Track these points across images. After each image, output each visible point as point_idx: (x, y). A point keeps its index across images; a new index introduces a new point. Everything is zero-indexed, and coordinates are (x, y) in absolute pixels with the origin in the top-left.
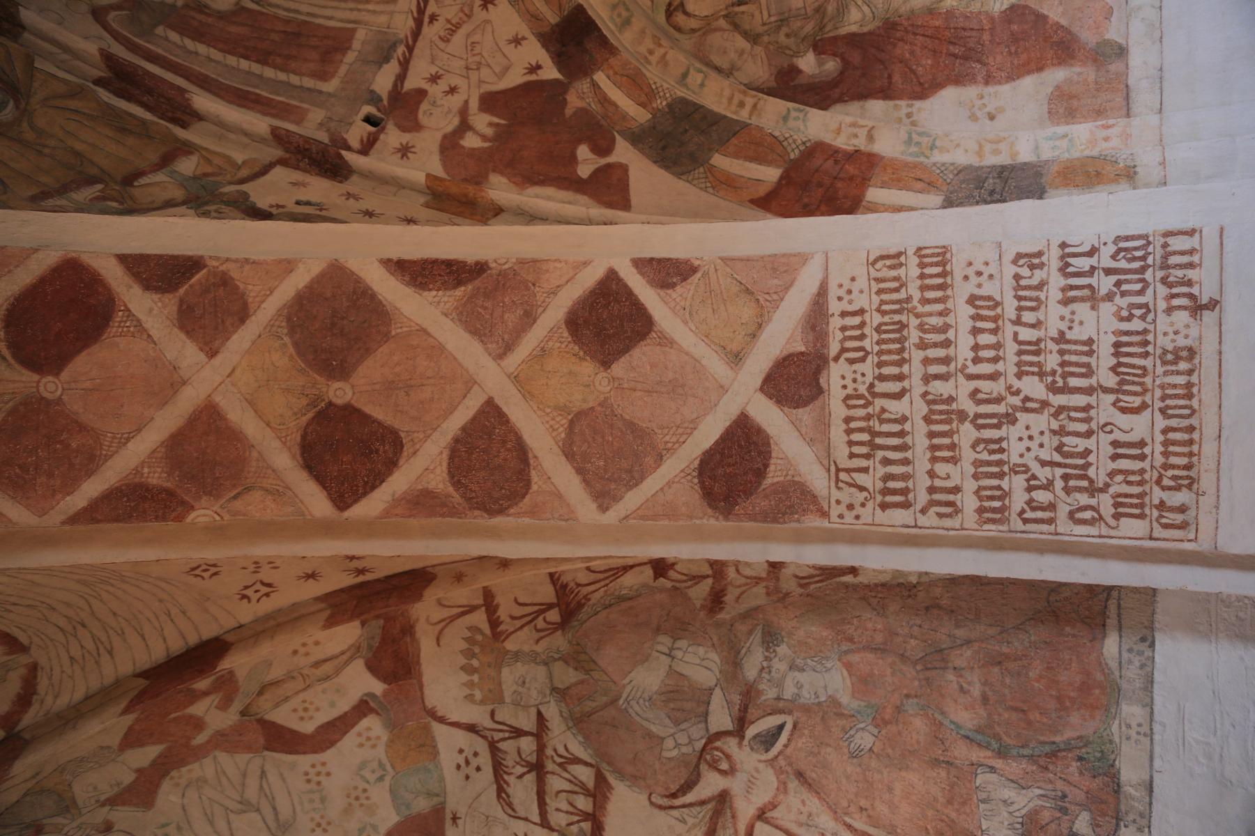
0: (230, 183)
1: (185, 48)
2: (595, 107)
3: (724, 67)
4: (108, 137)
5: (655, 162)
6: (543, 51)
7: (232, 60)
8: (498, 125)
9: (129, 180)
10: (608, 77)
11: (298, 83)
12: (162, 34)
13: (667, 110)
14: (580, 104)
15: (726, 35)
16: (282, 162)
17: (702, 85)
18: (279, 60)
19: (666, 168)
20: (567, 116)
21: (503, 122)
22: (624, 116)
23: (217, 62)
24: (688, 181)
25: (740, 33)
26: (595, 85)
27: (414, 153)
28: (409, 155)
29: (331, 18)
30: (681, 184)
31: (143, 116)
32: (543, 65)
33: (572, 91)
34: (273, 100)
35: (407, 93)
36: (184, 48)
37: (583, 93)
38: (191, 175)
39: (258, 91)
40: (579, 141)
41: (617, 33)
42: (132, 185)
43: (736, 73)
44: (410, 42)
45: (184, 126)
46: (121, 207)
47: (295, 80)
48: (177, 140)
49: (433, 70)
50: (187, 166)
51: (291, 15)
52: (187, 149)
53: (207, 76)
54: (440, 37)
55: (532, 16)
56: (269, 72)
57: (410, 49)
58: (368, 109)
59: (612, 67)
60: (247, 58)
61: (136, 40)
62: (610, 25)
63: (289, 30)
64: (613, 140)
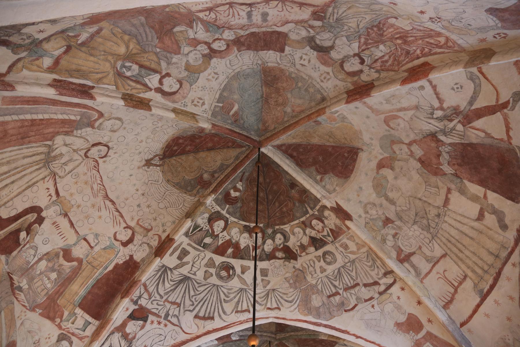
0: (24, 58)
1: (67, 115)
4: (83, 66)
7: (46, 116)
9: (69, 48)
11: (13, 116)
12: (77, 117)
16: (4, 75)
18: (26, 124)
23: (52, 113)
29: (11, 151)
31: (72, 79)
34: (21, 105)
36: (67, 114)
38: (44, 58)
39: (30, 106)
42: (67, 46)
45: (55, 80)
46: (68, 33)
47: (15, 117)
48: (55, 73)
50: (47, 62)
51: (29, 146)
52: (51, 70)
53: (54, 105)
56: (28, 117)
60: (41, 120)
61: (85, 110)
63: (27, 139)
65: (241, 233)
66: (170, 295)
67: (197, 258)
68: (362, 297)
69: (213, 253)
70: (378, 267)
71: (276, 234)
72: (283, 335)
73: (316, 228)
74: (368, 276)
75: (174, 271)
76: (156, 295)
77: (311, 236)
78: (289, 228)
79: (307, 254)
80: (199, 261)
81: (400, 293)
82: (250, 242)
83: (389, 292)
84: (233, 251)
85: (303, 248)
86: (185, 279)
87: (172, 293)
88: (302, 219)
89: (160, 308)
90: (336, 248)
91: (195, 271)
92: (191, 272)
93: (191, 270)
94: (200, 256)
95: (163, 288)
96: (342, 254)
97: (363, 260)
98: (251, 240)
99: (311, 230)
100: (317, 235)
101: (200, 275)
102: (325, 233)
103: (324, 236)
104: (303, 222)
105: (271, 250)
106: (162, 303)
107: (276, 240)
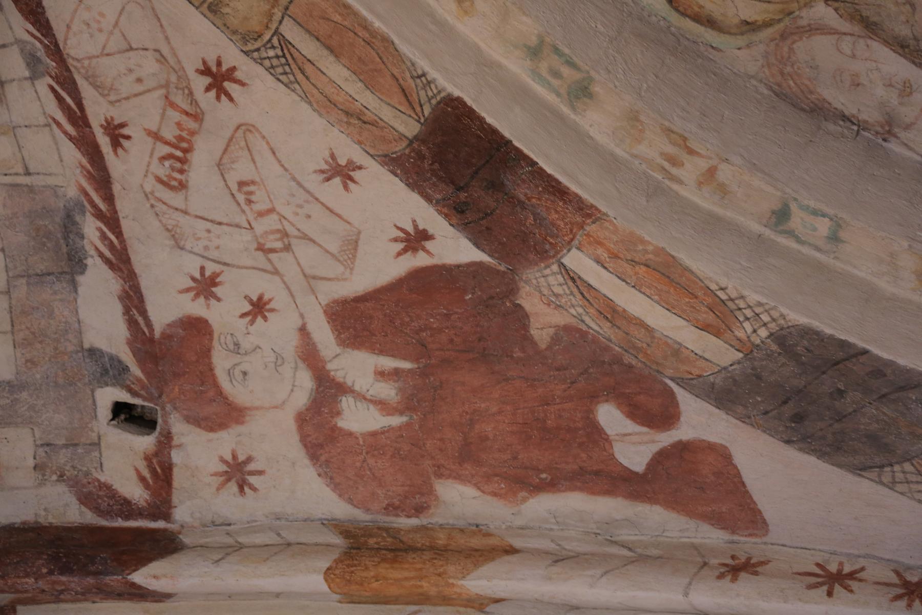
2: (595, 325)
3: (863, 116)
5: (788, 442)
6: (415, 199)
8: (396, 373)
10: (598, 261)
13: (774, 347)
14: (558, 319)
15: (846, 45)
17: (834, 238)
19: (821, 455)
20: (543, 346)
21: (406, 365)
22: (677, 351)
24: (881, 483)
25: (886, 43)
26: (573, 278)
27: (260, 473)
28: (252, 479)
30: (865, 486)
32: (431, 231)
33: (525, 289)
35: (166, 336)
37: (557, 296)
40: (594, 397)
41: (565, 110)
43: (902, 135)
44: (102, 206)
49: (192, 265)
54: (159, 180)
55: (347, 113)
57: (112, 221)
58: (108, 396)
59: (600, 243)
62: (538, 89)
64: (672, 394)
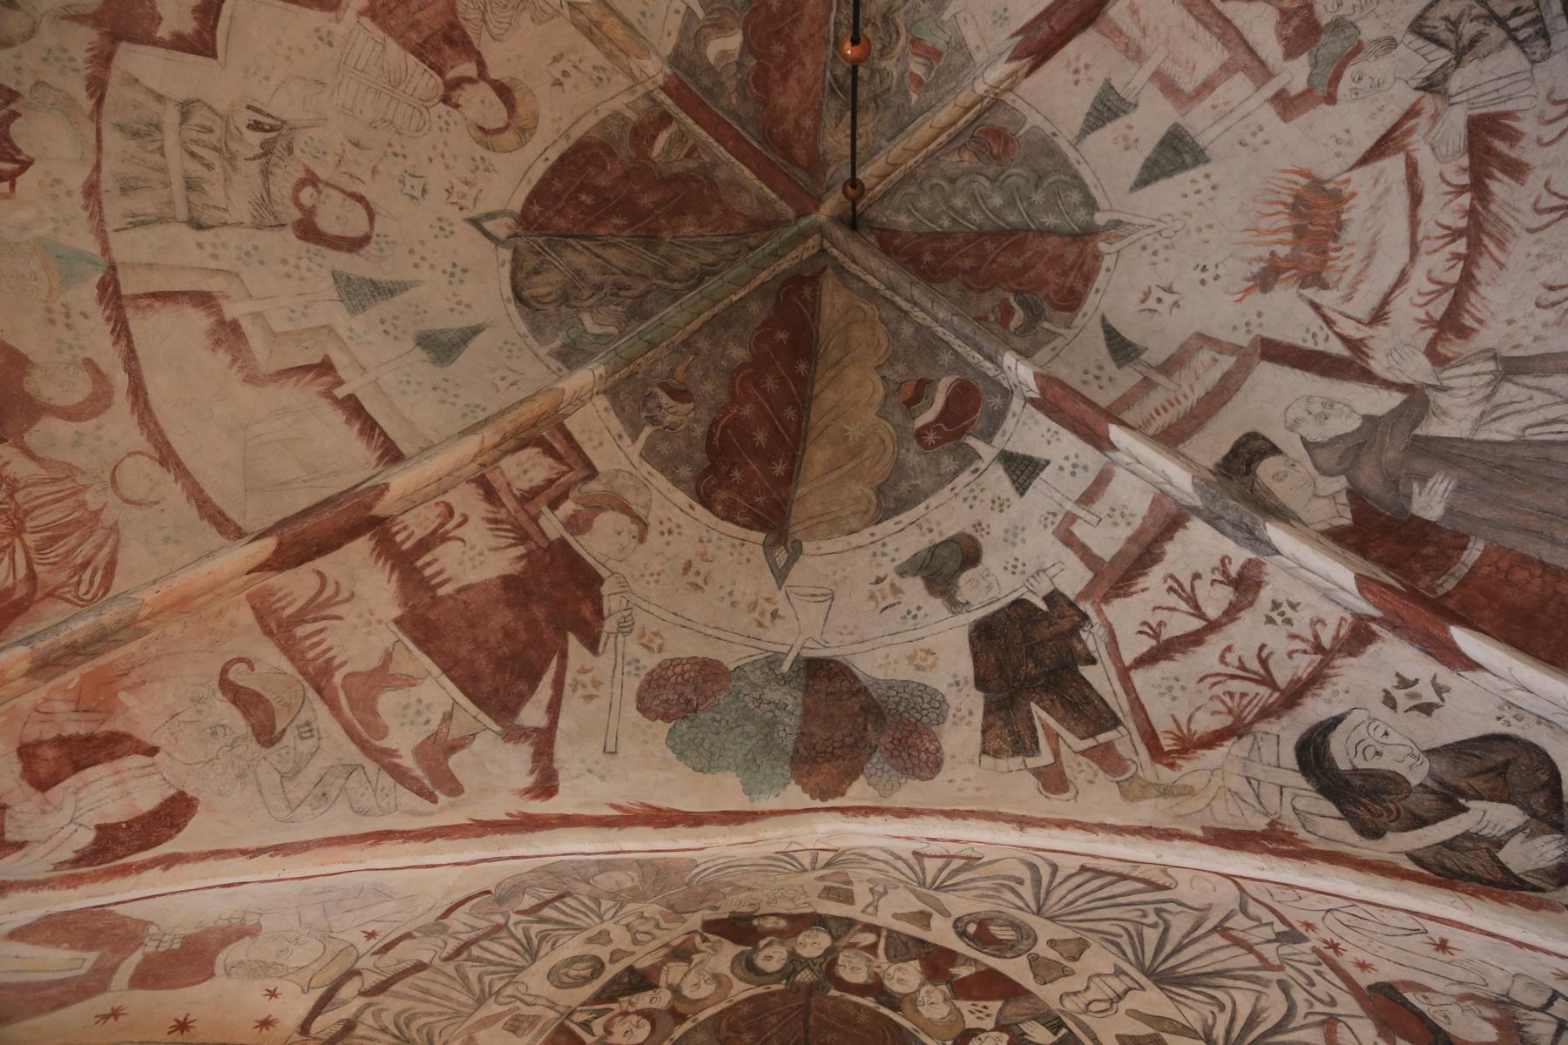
65: (912, 998)
66: (1245, 969)
67: (1094, 1007)
68: (427, 939)
69: (1027, 993)
70: (384, 1030)
71: (783, 968)
72: (785, 266)
73: (634, 1019)
74: (415, 993)
75: (1198, 1027)
76: (1302, 1008)
77: (651, 992)
78: (733, 992)
79: (666, 945)
80: (1089, 996)
81: (271, 1008)
82: (885, 966)
83: (317, 994)
84: (953, 967)
85: (682, 953)
86: (1166, 980)
87: (1234, 970)
88: (688, 1025)
89: (1309, 970)
90: (552, 1005)
91: (1117, 980)
92: (1132, 985)
93: (1131, 989)
94: (1083, 1006)
95: (1264, 1002)
96: (529, 999)
97: (443, 1024)
98: (876, 970)
99: (653, 1006)
100: (631, 1004)
101: (1099, 959)
102: (598, 1026)
103: (600, 1013)
104: (680, 1018)
105: (807, 933)
106: (1289, 970)
107: (785, 955)
